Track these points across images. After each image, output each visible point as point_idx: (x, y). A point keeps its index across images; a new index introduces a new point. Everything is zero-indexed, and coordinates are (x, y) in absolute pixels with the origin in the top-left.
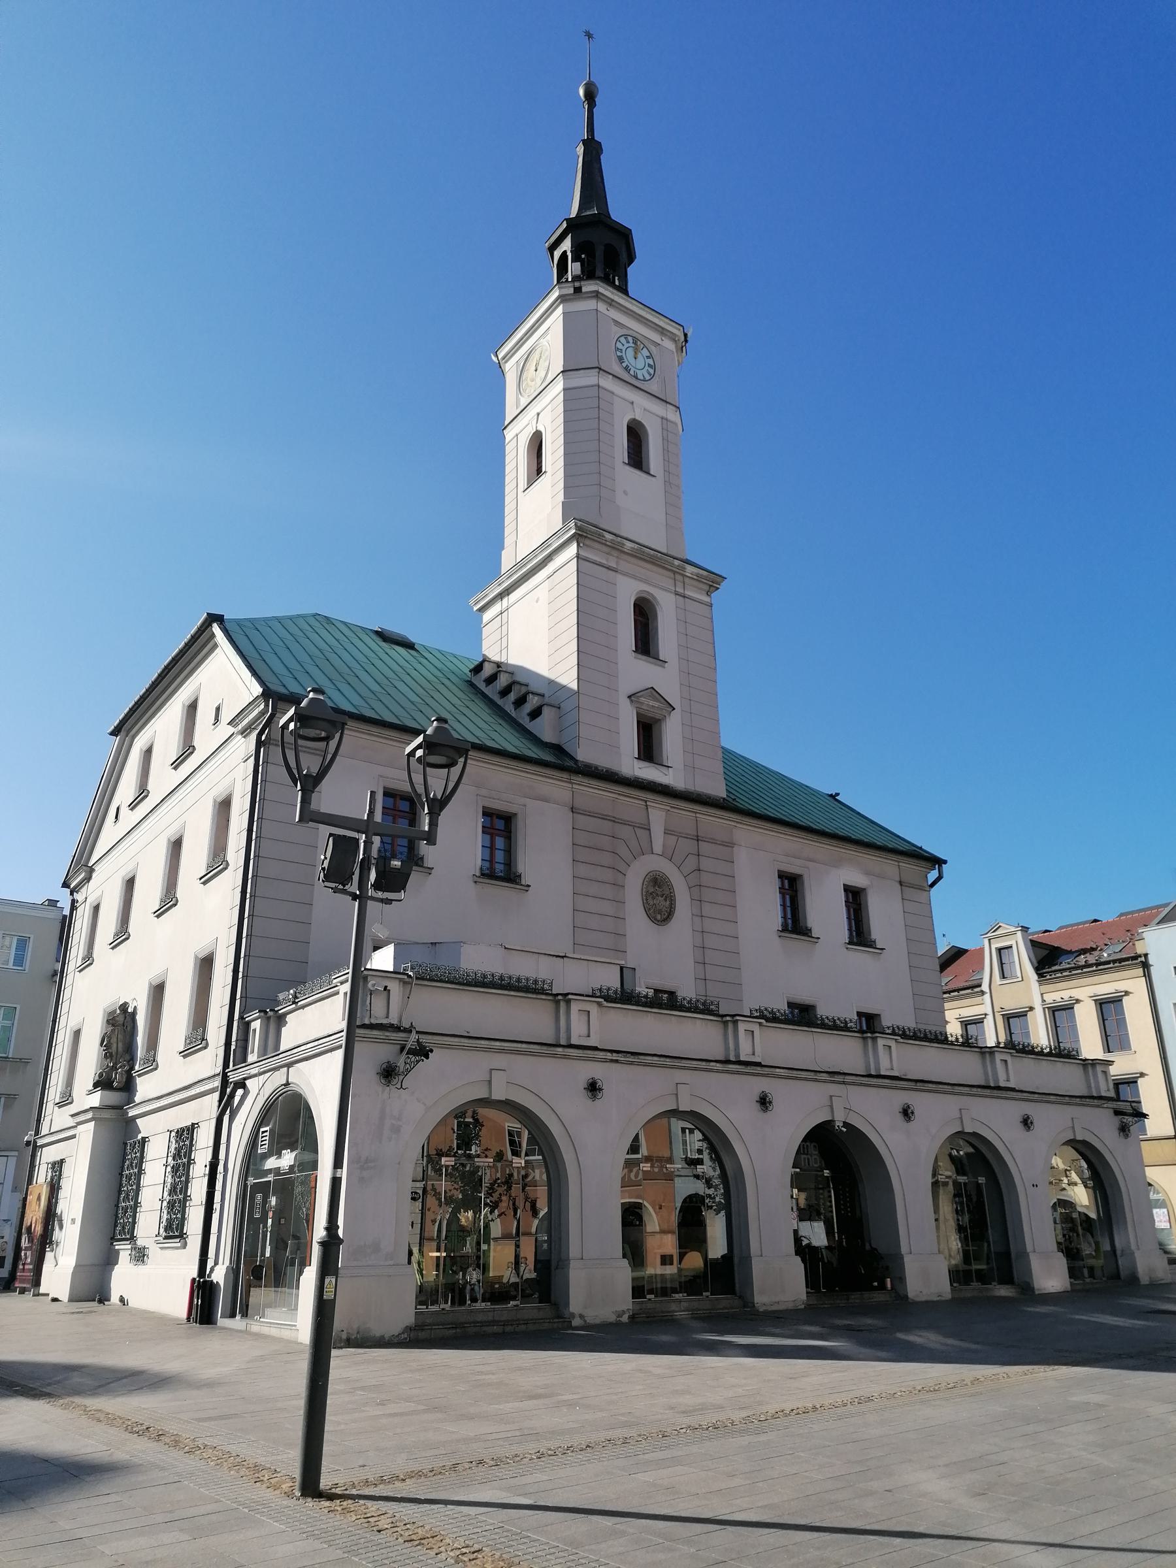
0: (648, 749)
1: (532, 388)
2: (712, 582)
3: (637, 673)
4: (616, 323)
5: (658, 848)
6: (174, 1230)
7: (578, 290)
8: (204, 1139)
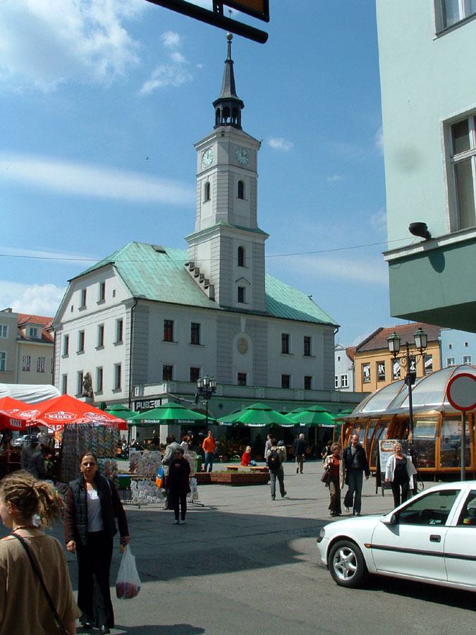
0: (241, 299)
1: (207, 161)
2: (266, 236)
3: (237, 271)
5: (243, 330)
7: (223, 135)
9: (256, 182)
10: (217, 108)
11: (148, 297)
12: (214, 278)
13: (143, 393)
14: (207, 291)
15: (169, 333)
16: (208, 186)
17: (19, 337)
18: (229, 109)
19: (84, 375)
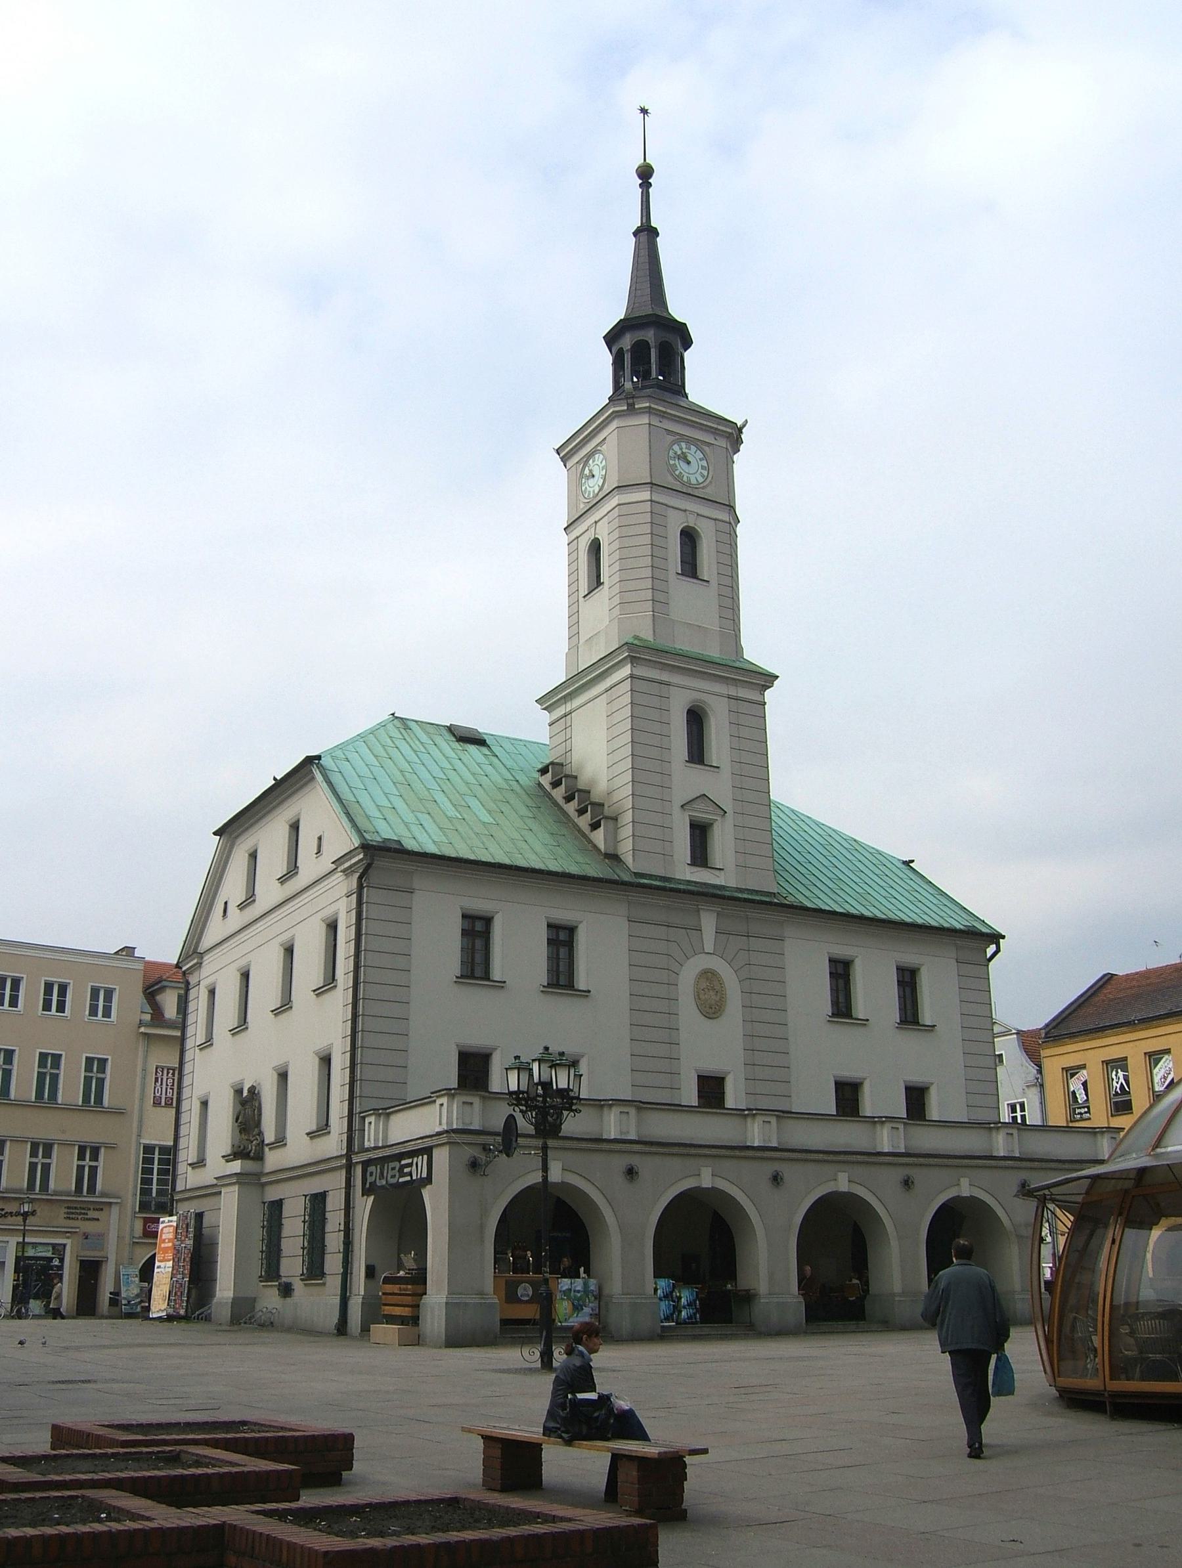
0: (700, 856)
3: (687, 781)
4: (669, 432)
5: (709, 947)
6: (315, 1270)
7: (631, 407)
8: (335, 1202)
9: (733, 535)
10: (614, 350)
11: (410, 844)
12: (617, 797)
13: (385, 1137)
14: (599, 837)
15: (478, 958)
16: (595, 547)
17: (148, 1017)
18: (649, 349)
19: (245, 1093)
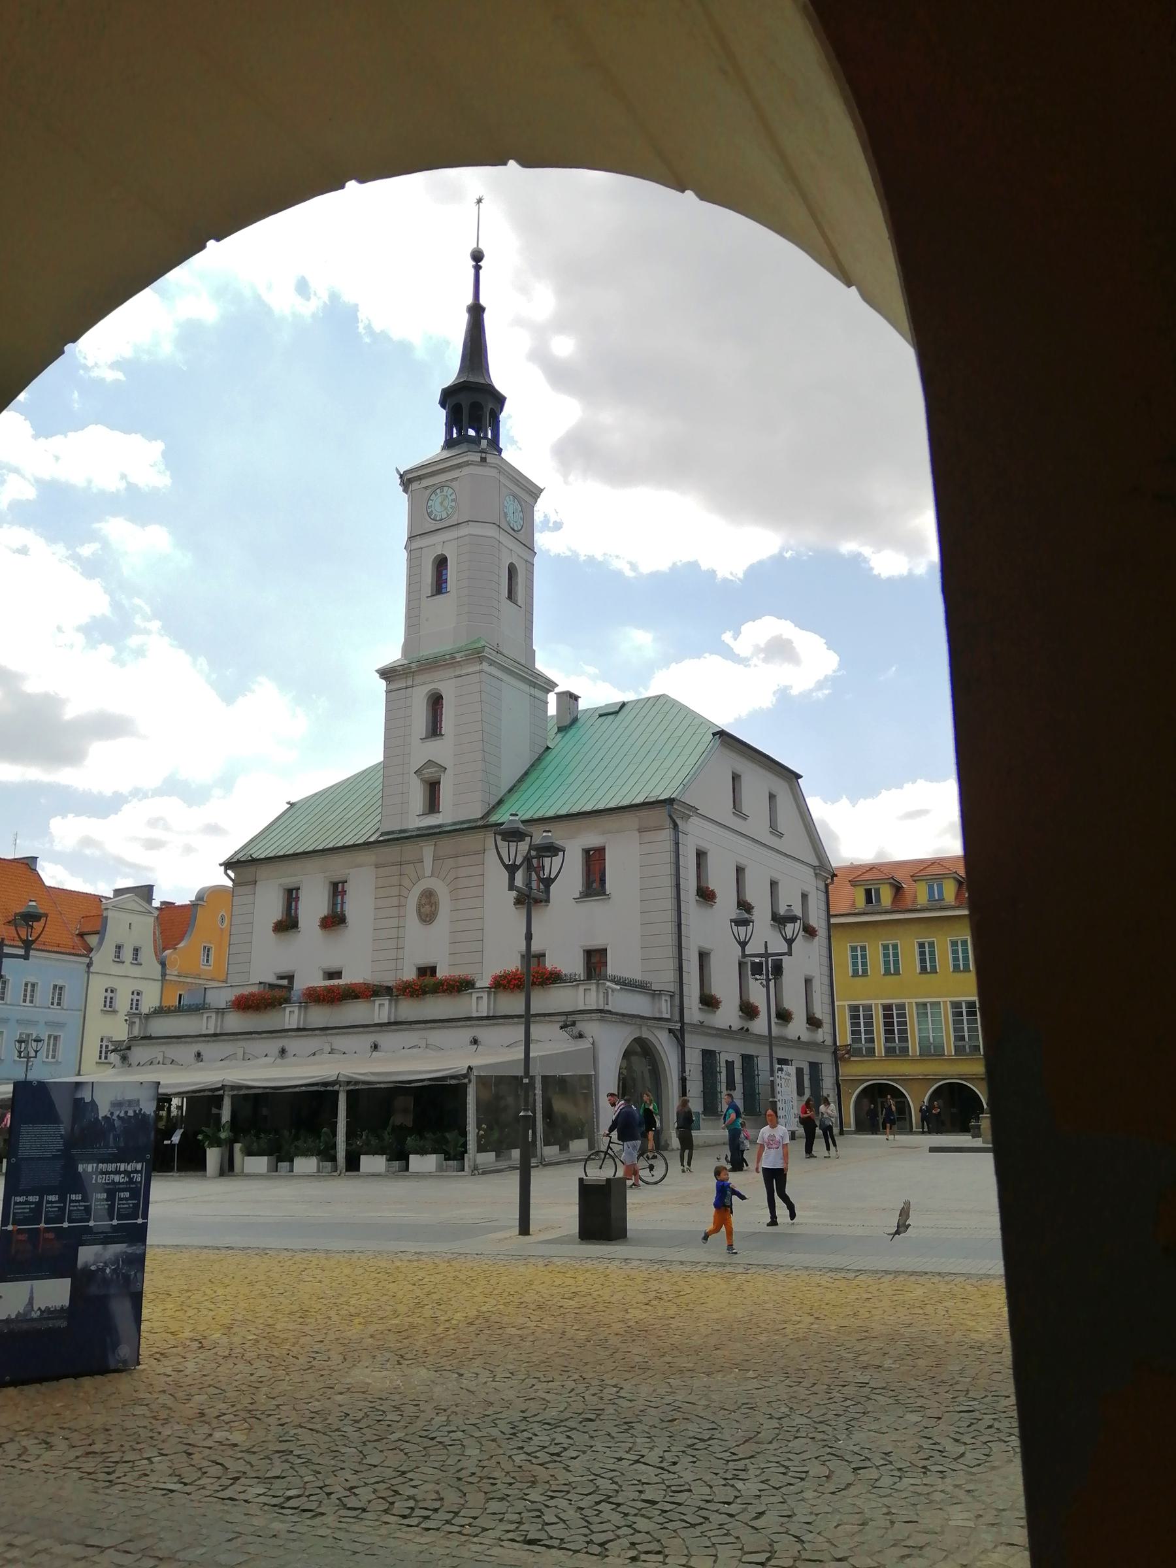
7: (483, 460)
16: (441, 563)
